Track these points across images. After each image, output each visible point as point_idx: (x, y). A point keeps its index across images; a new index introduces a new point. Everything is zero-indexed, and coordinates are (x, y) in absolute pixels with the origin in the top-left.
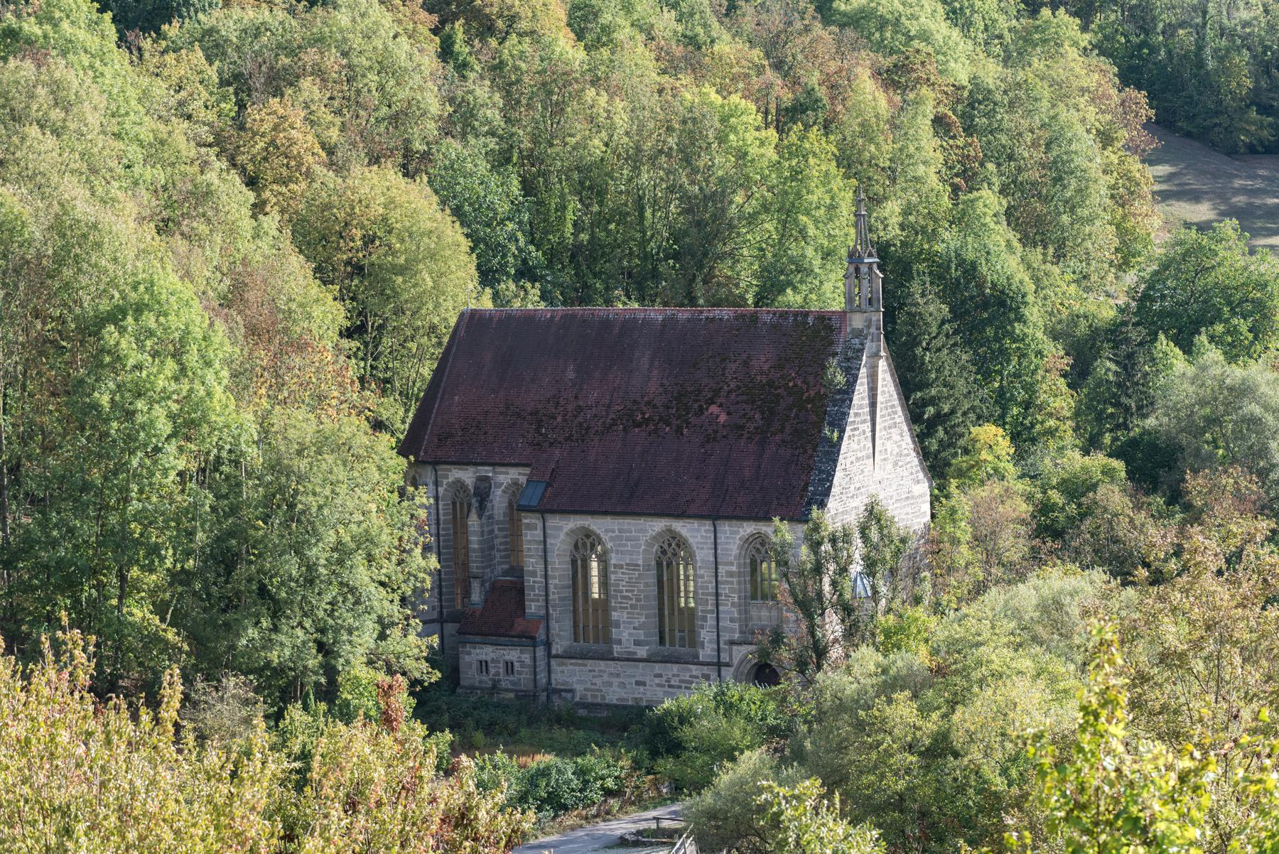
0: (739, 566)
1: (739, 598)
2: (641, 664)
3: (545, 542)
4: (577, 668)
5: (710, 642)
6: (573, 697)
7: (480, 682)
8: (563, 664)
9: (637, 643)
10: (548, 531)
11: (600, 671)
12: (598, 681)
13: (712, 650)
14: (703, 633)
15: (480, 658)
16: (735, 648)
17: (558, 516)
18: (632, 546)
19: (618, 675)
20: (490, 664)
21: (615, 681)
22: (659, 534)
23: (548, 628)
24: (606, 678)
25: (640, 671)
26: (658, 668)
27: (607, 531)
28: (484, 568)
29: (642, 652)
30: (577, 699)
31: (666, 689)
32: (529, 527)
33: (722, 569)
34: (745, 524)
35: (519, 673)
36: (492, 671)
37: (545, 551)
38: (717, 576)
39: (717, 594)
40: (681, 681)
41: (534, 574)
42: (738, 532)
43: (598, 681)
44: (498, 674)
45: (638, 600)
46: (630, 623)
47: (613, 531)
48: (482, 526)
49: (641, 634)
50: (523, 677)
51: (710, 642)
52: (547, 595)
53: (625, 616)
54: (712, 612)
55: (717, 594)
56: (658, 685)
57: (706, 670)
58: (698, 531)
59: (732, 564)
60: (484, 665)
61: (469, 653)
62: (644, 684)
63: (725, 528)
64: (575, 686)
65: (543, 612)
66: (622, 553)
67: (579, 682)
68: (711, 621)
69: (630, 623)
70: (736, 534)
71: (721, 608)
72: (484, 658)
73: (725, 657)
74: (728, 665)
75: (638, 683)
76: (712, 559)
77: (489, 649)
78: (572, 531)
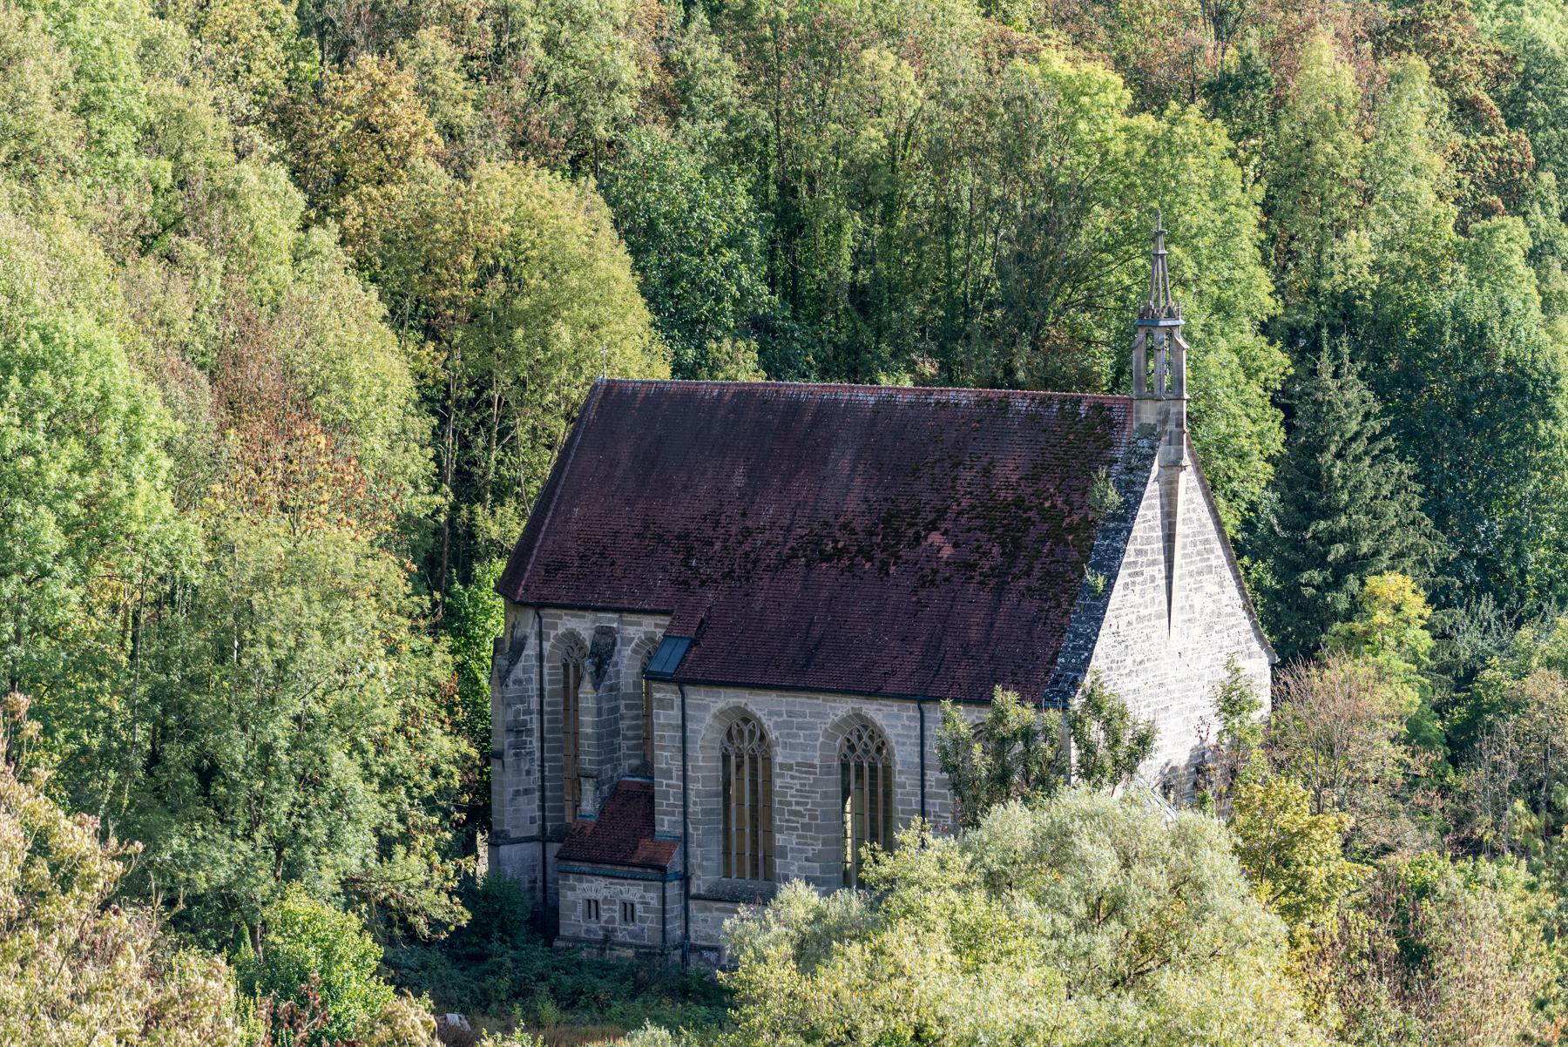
7: (588, 931)
8: (706, 909)
15: (588, 895)
20: (601, 906)
22: (844, 720)
23: (686, 855)
27: (771, 714)
28: (600, 763)
35: (642, 920)
36: (604, 915)
38: (923, 786)
44: (611, 920)
47: (780, 714)
52: (685, 806)
58: (898, 717)
60: (593, 907)
65: (679, 831)
66: (792, 747)
72: (593, 895)
77: (601, 883)
78: (722, 712)
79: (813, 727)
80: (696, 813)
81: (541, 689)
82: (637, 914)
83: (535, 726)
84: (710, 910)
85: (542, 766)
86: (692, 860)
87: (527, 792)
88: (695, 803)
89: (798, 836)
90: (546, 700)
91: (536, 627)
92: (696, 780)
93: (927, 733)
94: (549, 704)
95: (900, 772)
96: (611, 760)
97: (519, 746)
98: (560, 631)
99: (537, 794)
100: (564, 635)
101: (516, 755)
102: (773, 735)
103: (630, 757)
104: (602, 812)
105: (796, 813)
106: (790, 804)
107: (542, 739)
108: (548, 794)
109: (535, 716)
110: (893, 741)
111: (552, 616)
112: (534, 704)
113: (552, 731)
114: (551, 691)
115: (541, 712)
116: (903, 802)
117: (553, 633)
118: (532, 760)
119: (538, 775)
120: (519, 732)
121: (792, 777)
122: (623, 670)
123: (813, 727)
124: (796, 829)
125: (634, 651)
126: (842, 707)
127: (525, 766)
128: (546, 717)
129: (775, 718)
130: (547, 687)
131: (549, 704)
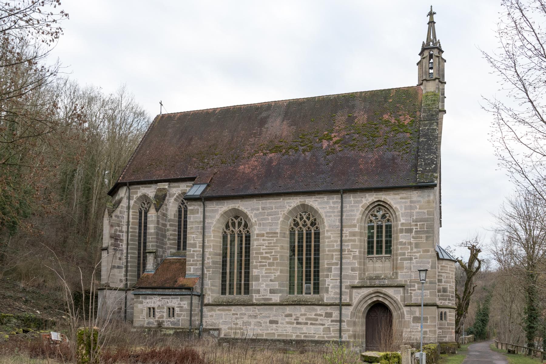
0: (361, 227)
1: (360, 252)
2: (275, 307)
4: (223, 313)
5: (333, 287)
6: (219, 334)
7: (148, 323)
8: (212, 310)
9: (272, 292)
10: (207, 214)
11: (241, 314)
12: (240, 322)
13: (335, 293)
14: (328, 281)
15: (149, 306)
16: (355, 291)
17: (215, 203)
19: (255, 317)
20: (156, 310)
22: (294, 209)
23: (202, 284)
24: (246, 319)
26: (288, 310)
28: (157, 246)
29: (276, 298)
30: (222, 336)
31: (295, 325)
32: (194, 212)
33: (346, 231)
34: (367, 195)
35: (179, 315)
36: (158, 315)
37: (204, 228)
38: (341, 236)
39: (341, 250)
40: (307, 319)
41: (194, 246)
42: (361, 202)
43: (240, 322)
44: (162, 317)
46: (267, 277)
47: (258, 209)
48: (158, 217)
49: (276, 285)
50: (182, 319)
51: (333, 287)
52: (203, 260)
53: (264, 272)
54: (337, 264)
55: (341, 250)
56: (288, 323)
57: (329, 309)
58: (327, 203)
59: (355, 226)
60: (152, 311)
61: (141, 303)
62: (276, 322)
63: (350, 199)
65: (199, 273)
67: (225, 323)
68: (335, 271)
69: (267, 277)
70: (357, 206)
71: (344, 261)
72: (152, 305)
73: (346, 299)
74: (349, 305)
75: (271, 322)
76: (338, 223)
77: (157, 298)
78: (225, 213)
79: (276, 213)
80: (209, 263)
81: (128, 222)
82: (176, 312)
83: (125, 238)
84: (215, 311)
85: (127, 256)
86: (205, 287)
87: (119, 267)
88: (208, 258)
89: (266, 269)
90: (131, 226)
91: (127, 194)
92: (209, 247)
93: (344, 209)
94: (132, 228)
95: (327, 231)
96: (162, 248)
97: (116, 247)
98: (139, 194)
99: (124, 269)
100: (141, 197)
101: (114, 249)
102: (253, 220)
103: (171, 248)
104: (157, 269)
105: (265, 258)
106: (262, 253)
107: (128, 244)
108: (129, 269)
109: (125, 234)
110: (323, 215)
111: (135, 188)
112: (124, 229)
113: (132, 240)
114: (132, 222)
115: (128, 232)
117: (135, 196)
118: (122, 254)
119: (125, 261)
120: (116, 240)
121: (264, 240)
122: (170, 209)
124: (265, 265)
125: (175, 200)
126: (294, 202)
127: (119, 256)
128: (130, 234)
129: (255, 212)
130: (131, 220)
131: (132, 228)
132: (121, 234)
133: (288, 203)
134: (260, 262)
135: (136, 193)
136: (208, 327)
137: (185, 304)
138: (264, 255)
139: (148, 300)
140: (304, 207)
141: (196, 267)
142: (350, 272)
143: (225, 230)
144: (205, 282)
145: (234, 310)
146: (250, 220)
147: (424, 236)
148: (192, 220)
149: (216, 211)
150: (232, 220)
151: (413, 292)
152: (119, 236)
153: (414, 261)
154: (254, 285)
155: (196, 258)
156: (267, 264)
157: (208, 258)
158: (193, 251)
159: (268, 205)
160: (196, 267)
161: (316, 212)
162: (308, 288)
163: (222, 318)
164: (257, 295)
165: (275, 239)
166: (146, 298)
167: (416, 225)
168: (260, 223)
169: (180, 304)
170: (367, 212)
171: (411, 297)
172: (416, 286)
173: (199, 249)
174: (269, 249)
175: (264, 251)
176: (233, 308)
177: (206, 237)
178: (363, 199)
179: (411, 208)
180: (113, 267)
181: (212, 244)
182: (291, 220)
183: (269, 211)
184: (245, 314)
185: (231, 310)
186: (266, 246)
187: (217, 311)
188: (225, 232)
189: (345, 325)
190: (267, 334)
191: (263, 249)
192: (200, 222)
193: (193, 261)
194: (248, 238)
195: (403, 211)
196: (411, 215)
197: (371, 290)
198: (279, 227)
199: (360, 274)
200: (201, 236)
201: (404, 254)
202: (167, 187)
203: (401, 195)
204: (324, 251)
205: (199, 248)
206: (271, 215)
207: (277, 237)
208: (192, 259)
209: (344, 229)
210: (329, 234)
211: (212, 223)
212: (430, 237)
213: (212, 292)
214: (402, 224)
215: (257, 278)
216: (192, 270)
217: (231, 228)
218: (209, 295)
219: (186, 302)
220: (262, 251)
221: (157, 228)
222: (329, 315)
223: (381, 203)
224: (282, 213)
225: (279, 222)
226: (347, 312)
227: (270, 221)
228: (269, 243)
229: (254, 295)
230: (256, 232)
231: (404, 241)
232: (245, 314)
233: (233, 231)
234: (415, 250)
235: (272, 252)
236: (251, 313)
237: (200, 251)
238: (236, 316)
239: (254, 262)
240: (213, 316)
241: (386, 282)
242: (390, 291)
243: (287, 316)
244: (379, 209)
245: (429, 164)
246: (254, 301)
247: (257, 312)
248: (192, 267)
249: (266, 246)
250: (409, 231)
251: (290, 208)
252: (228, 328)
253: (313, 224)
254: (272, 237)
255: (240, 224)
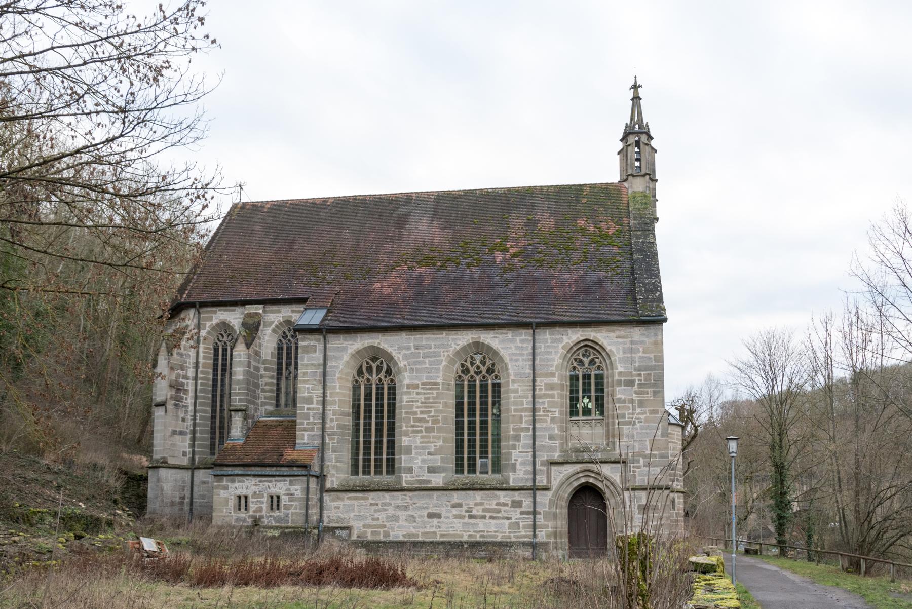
0: (561, 377)
1: (561, 413)
2: (436, 494)
3: (325, 364)
4: (355, 503)
6: (350, 535)
7: (237, 520)
8: (339, 499)
9: (432, 470)
10: (329, 353)
11: (384, 504)
12: (382, 516)
13: (526, 472)
14: (515, 454)
15: (238, 493)
16: (554, 468)
17: (341, 337)
18: (430, 363)
19: (406, 508)
20: (250, 499)
21: (402, 514)
22: (464, 349)
23: (322, 459)
24: (391, 511)
25: (433, 502)
26: (456, 497)
27: (400, 348)
28: (248, 401)
29: (438, 480)
31: (466, 520)
32: (307, 350)
34: (570, 331)
35: (287, 507)
36: (253, 506)
37: (324, 374)
38: (534, 390)
39: (534, 410)
40: (484, 510)
42: (561, 340)
43: (382, 516)
44: (260, 510)
45: (436, 422)
46: (423, 448)
47: (409, 348)
48: (249, 356)
49: (437, 461)
50: (292, 513)
52: (324, 423)
53: (418, 440)
54: (527, 429)
55: (534, 410)
56: (456, 517)
57: (517, 496)
58: (512, 341)
59: (553, 375)
60: (242, 501)
61: (226, 488)
62: (438, 516)
63: (546, 337)
64: (352, 523)
65: (317, 442)
66: (418, 370)
67: (359, 518)
68: (525, 439)
69: (423, 448)
70: (557, 346)
71: (537, 425)
72: (243, 492)
73: (541, 480)
74: (546, 489)
75: (430, 516)
76: (529, 371)
77: (253, 481)
78: (358, 352)
79: (436, 355)
80: (332, 427)
81: (197, 363)
82: (282, 503)
83: (190, 387)
84: (342, 500)
85: (195, 416)
86: (327, 463)
87: (182, 433)
88: (332, 420)
89: (422, 437)
90: (200, 369)
91: (196, 321)
92: (334, 403)
93: (537, 351)
94: (202, 372)
95: (513, 381)
96: (254, 403)
97: (178, 399)
98: (215, 321)
99: (189, 436)
100: (217, 325)
101: (176, 405)
102: (402, 364)
103: (266, 404)
104: (247, 437)
105: (420, 420)
106: (416, 413)
107: (196, 397)
108: (198, 435)
109: (191, 382)
110: (507, 359)
111: (209, 312)
112: (191, 373)
113: (202, 391)
114: (204, 364)
115: (196, 379)
116: (515, 404)
117: (208, 324)
118: (186, 412)
119: (190, 422)
120: (178, 390)
121: (418, 393)
122: (265, 344)
123: (436, 355)
124: (421, 431)
125: (274, 331)
126: (464, 338)
127: (182, 415)
128: (199, 382)
129: (404, 351)
130: (201, 360)
131: (202, 372)
132: (185, 381)
133: (454, 340)
134: (413, 426)
135: (211, 319)
136: (331, 525)
137: (298, 489)
138: (419, 416)
139: (237, 485)
140: (478, 347)
141: (312, 433)
142: (547, 442)
143: (357, 378)
144: (326, 455)
145: (373, 499)
146: (396, 364)
147: (650, 390)
148: (305, 362)
149: (344, 349)
150: (367, 363)
151: (637, 470)
152: (183, 384)
153: (638, 425)
154: (403, 460)
155: (311, 419)
156: (423, 429)
157: (332, 420)
158: (308, 409)
159: (424, 343)
160: (312, 433)
161: (496, 353)
162: (484, 465)
163: (353, 511)
164: (409, 475)
165: (435, 392)
166: (233, 482)
167: (640, 375)
168: (413, 369)
169: (290, 490)
170: (569, 355)
171: (634, 476)
172: (642, 460)
173: (316, 406)
174: (426, 407)
175: (418, 410)
176: (372, 495)
177: (327, 388)
178: (564, 337)
179: (632, 351)
180: (174, 432)
181: (337, 399)
182: (458, 365)
183: (426, 351)
184: (390, 504)
185: (367, 499)
186: (422, 403)
187: (346, 500)
188: (357, 381)
189: (540, 519)
190: (424, 534)
191: (418, 407)
192: (319, 365)
193: (308, 423)
194: (392, 391)
195: (621, 355)
196: (632, 361)
197: (578, 467)
198: (441, 374)
199: (562, 445)
200: (320, 387)
201: (623, 416)
202: (261, 311)
203: (618, 333)
204: (508, 410)
205: (317, 404)
206: (429, 357)
207: (438, 389)
208: (305, 422)
209: (538, 379)
210: (516, 385)
211: (338, 367)
212: (659, 391)
213: (338, 470)
214: (620, 373)
215: (408, 451)
216: (306, 437)
217: (366, 375)
218: (333, 476)
219: (298, 487)
220: (415, 410)
221: (247, 373)
222: (517, 504)
223: (590, 344)
224: (446, 354)
225: (441, 367)
226: (544, 498)
227: (427, 366)
228: (425, 398)
229: (403, 475)
230: (407, 381)
231: (623, 397)
232: (390, 504)
233: (368, 380)
234: (638, 410)
235: (430, 412)
236: (399, 502)
237: (318, 409)
238: (376, 507)
239: (402, 426)
240: (339, 508)
241: (599, 456)
242: (606, 469)
243: (454, 506)
244: (586, 351)
245: (651, 290)
246: (404, 485)
247: (409, 500)
248: (306, 433)
249: (422, 403)
250: (630, 383)
251: (458, 348)
252: (364, 526)
253: (490, 371)
254: (430, 389)
255: (379, 369)
